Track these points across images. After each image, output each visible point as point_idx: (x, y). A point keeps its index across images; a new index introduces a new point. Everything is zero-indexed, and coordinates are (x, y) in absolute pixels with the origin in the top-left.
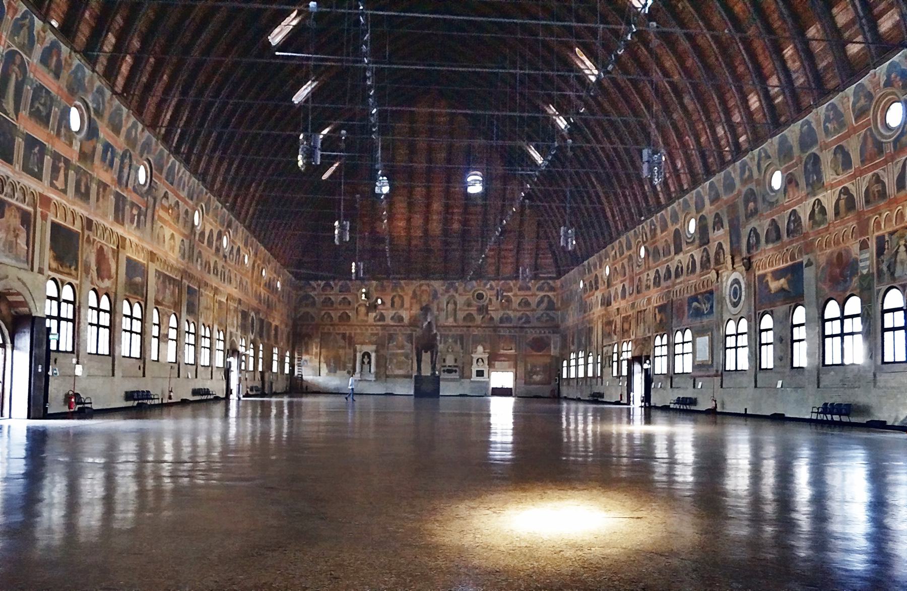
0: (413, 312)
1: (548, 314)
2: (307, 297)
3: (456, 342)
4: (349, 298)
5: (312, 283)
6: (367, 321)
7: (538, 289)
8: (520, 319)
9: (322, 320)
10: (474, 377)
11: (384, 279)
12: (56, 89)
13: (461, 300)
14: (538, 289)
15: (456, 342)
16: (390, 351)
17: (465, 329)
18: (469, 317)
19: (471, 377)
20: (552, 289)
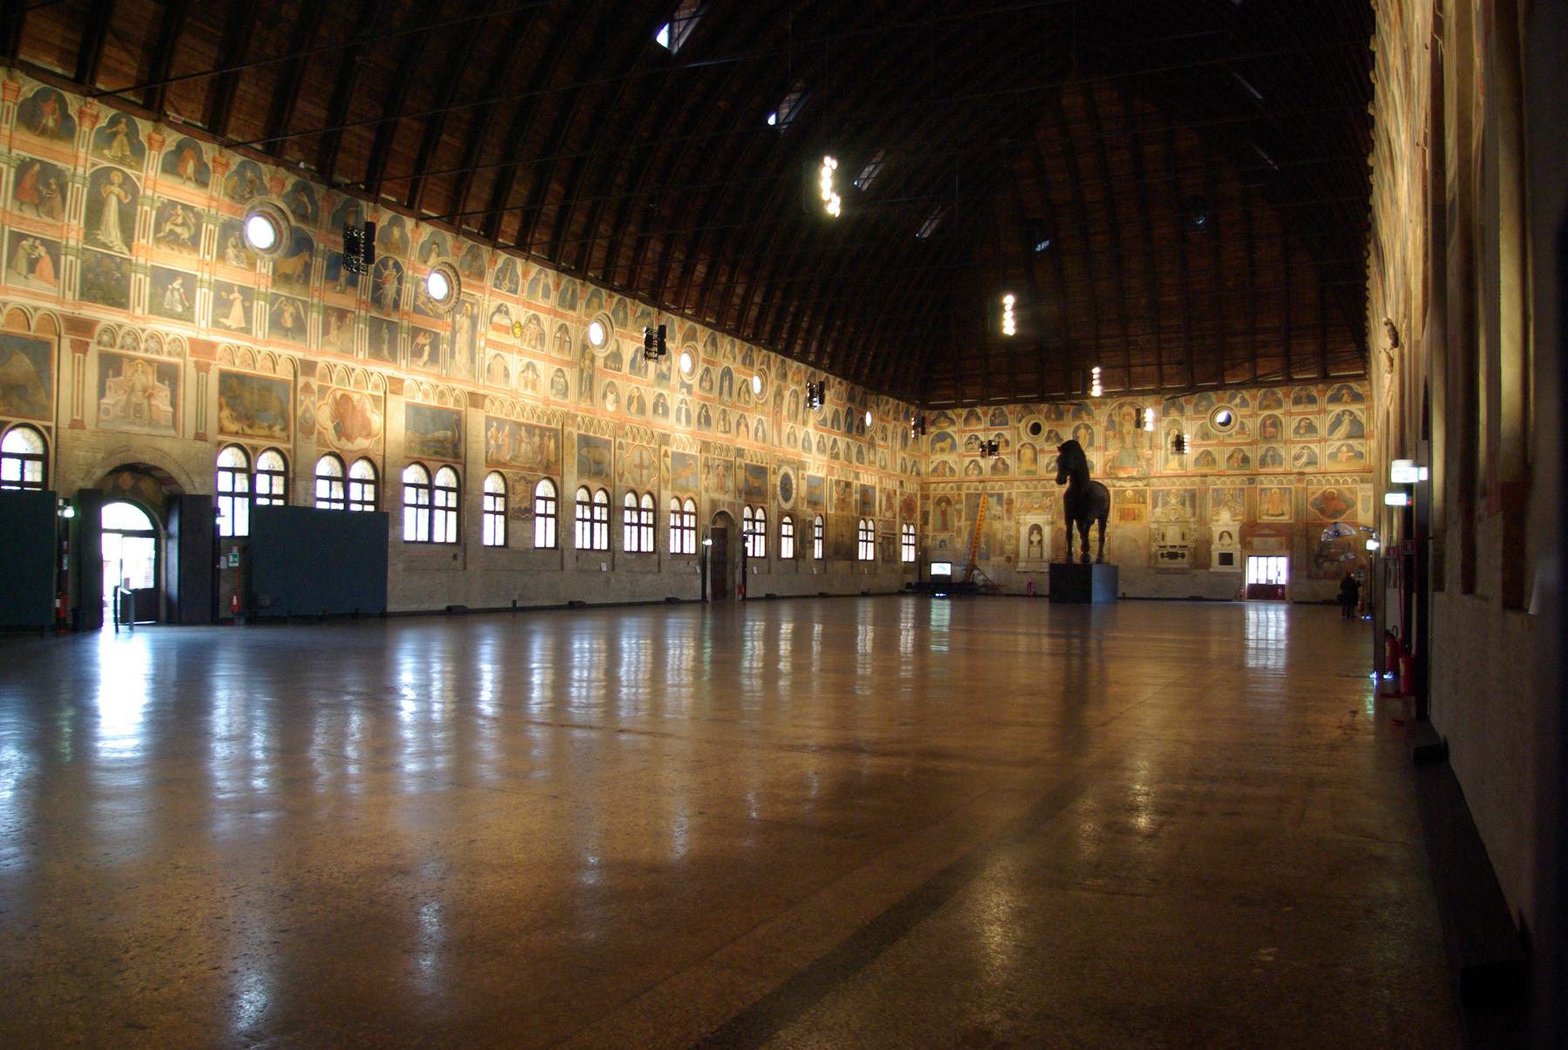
0: (1111, 453)
1: (1350, 448)
8: (1297, 458)
11: (1061, 398)
12: (205, 202)
17: (1197, 480)
20: (1357, 398)
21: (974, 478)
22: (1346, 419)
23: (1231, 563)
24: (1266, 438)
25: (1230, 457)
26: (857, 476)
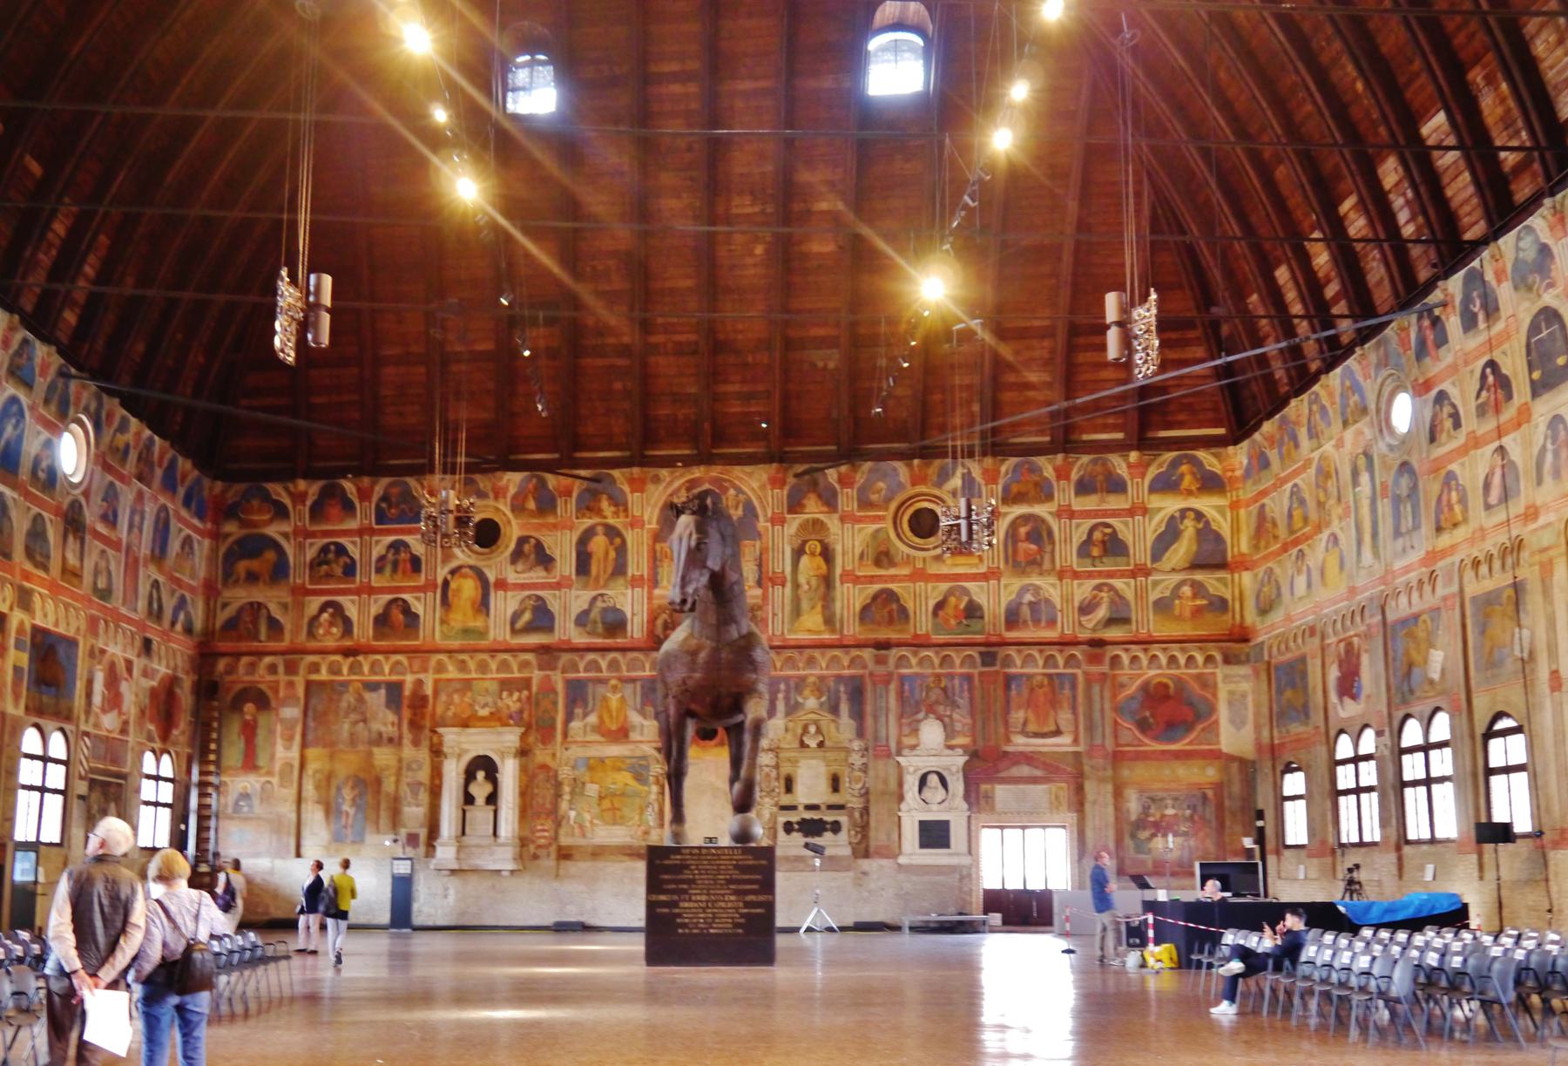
2: (254, 546)
3: (834, 710)
4: (417, 545)
5: (278, 491)
6: (482, 634)
8: (1086, 609)
9: (311, 634)
11: (550, 467)
13: (850, 540)
14: (1154, 488)
15: (834, 710)
16: (575, 752)
17: (867, 654)
18: (886, 606)
19: (891, 852)
20: (1211, 483)
21: (330, 643)
22: (1189, 527)
23: (924, 844)
24: (1020, 565)
25: (940, 606)
26: (24, 600)
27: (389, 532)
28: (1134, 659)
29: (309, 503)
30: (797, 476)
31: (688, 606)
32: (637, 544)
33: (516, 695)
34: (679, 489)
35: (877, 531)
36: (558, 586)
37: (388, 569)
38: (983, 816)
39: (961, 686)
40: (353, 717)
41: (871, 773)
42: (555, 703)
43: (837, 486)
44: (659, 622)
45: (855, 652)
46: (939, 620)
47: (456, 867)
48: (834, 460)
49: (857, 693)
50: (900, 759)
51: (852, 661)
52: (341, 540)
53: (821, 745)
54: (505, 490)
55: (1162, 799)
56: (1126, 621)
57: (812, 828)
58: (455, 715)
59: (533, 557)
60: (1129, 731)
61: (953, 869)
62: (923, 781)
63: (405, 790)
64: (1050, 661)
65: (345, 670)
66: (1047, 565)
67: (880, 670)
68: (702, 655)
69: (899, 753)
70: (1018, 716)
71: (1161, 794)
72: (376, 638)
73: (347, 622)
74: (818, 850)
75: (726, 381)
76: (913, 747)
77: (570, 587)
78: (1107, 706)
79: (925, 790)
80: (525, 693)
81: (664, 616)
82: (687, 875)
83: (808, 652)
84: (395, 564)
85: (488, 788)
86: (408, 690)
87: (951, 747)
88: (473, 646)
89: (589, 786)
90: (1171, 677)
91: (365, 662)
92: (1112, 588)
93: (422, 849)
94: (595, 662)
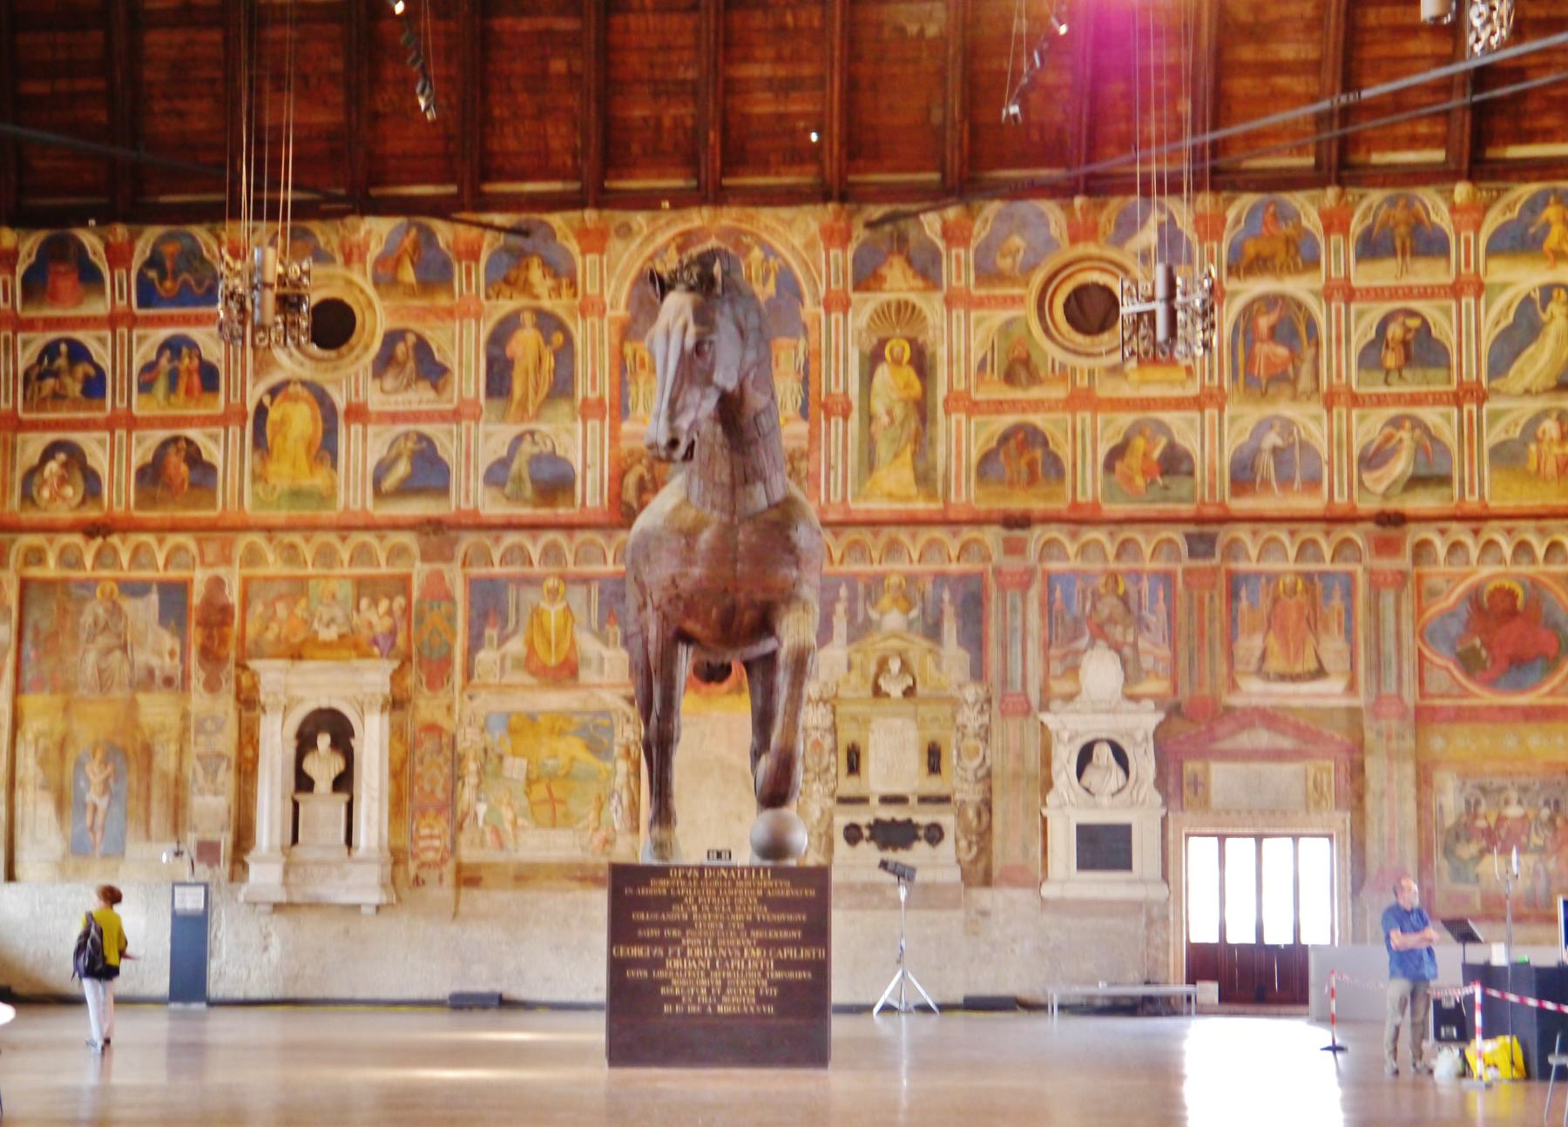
3: (933, 632)
4: (211, 346)
6: (325, 498)
7: (1493, 251)
8: (1373, 459)
9: (28, 497)
10: (1065, 875)
11: (442, 209)
13: (962, 337)
14: (1493, 251)
15: (933, 632)
16: (486, 703)
17: (992, 537)
19: (1032, 877)
21: (63, 513)
24: (1263, 382)
27: (161, 321)
28: (1455, 547)
29: (20, 269)
30: (870, 225)
31: (682, 450)
32: (593, 343)
33: (384, 605)
34: (666, 248)
35: (1009, 323)
36: (456, 416)
37: (161, 386)
38: (1188, 816)
39: (1153, 592)
40: (102, 641)
41: (996, 740)
42: (451, 618)
43: (941, 244)
44: (631, 480)
45: (968, 533)
46: (1116, 478)
47: (281, 897)
48: (937, 196)
49: (973, 605)
50: (1046, 718)
51: (964, 548)
52: (79, 335)
53: (909, 692)
54: (363, 250)
55: (1501, 790)
56: (1444, 480)
57: (894, 835)
58: (278, 638)
59: (411, 365)
60: (1444, 673)
61: (1136, 907)
62: (1085, 757)
63: (192, 766)
64: (1307, 549)
65: (88, 560)
66: (1305, 382)
67: (1013, 564)
68: (706, 538)
69: (1045, 707)
70: (1250, 645)
71: (1498, 782)
72: (140, 505)
73: (91, 479)
74: (903, 873)
75: (747, 59)
76: (1070, 698)
77: (476, 418)
78: (1407, 628)
79: (1089, 773)
80: (400, 601)
81: (640, 470)
82: (678, 913)
83: (888, 532)
84: (173, 377)
85: (338, 764)
86: (196, 599)
87: (1135, 698)
88: (310, 522)
89: (509, 761)
90: (1518, 578)
91: (123, 546)
92: (1418, 423)
93: (224, 869)
94: (521, 548)
